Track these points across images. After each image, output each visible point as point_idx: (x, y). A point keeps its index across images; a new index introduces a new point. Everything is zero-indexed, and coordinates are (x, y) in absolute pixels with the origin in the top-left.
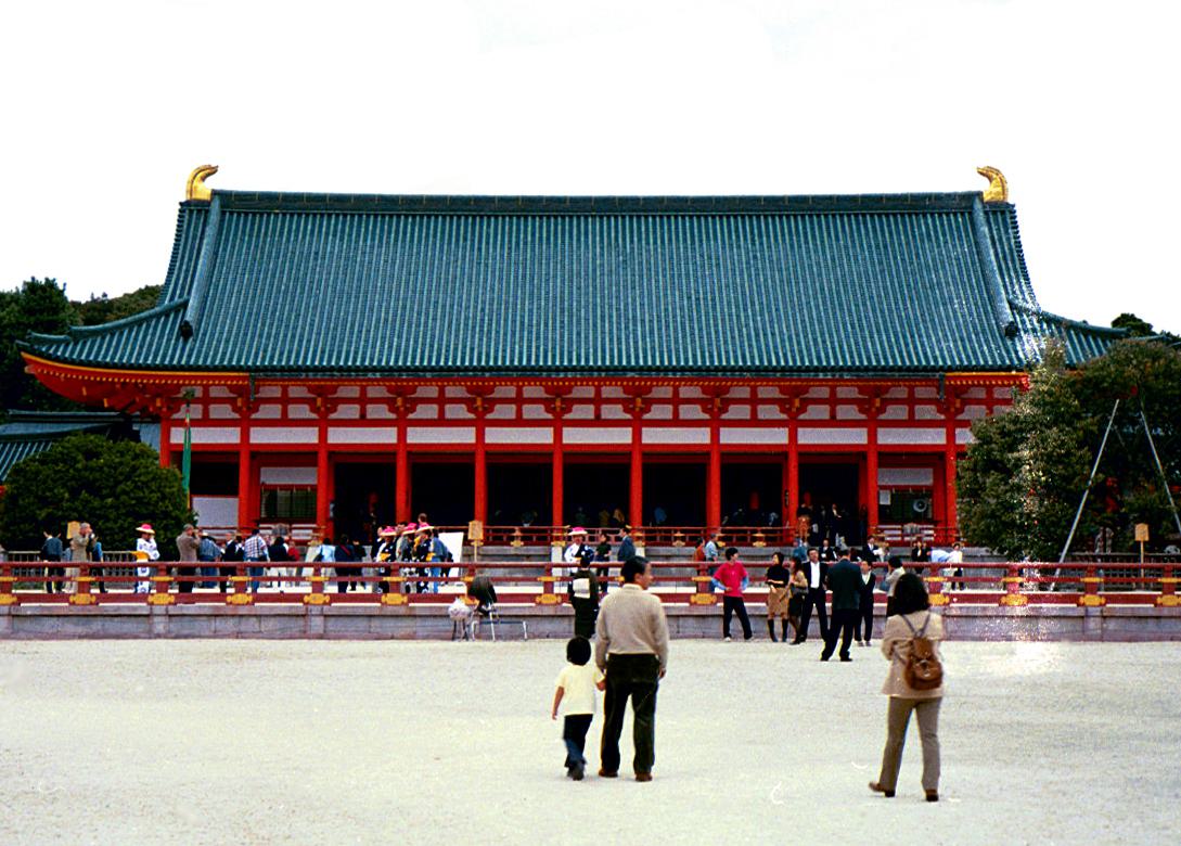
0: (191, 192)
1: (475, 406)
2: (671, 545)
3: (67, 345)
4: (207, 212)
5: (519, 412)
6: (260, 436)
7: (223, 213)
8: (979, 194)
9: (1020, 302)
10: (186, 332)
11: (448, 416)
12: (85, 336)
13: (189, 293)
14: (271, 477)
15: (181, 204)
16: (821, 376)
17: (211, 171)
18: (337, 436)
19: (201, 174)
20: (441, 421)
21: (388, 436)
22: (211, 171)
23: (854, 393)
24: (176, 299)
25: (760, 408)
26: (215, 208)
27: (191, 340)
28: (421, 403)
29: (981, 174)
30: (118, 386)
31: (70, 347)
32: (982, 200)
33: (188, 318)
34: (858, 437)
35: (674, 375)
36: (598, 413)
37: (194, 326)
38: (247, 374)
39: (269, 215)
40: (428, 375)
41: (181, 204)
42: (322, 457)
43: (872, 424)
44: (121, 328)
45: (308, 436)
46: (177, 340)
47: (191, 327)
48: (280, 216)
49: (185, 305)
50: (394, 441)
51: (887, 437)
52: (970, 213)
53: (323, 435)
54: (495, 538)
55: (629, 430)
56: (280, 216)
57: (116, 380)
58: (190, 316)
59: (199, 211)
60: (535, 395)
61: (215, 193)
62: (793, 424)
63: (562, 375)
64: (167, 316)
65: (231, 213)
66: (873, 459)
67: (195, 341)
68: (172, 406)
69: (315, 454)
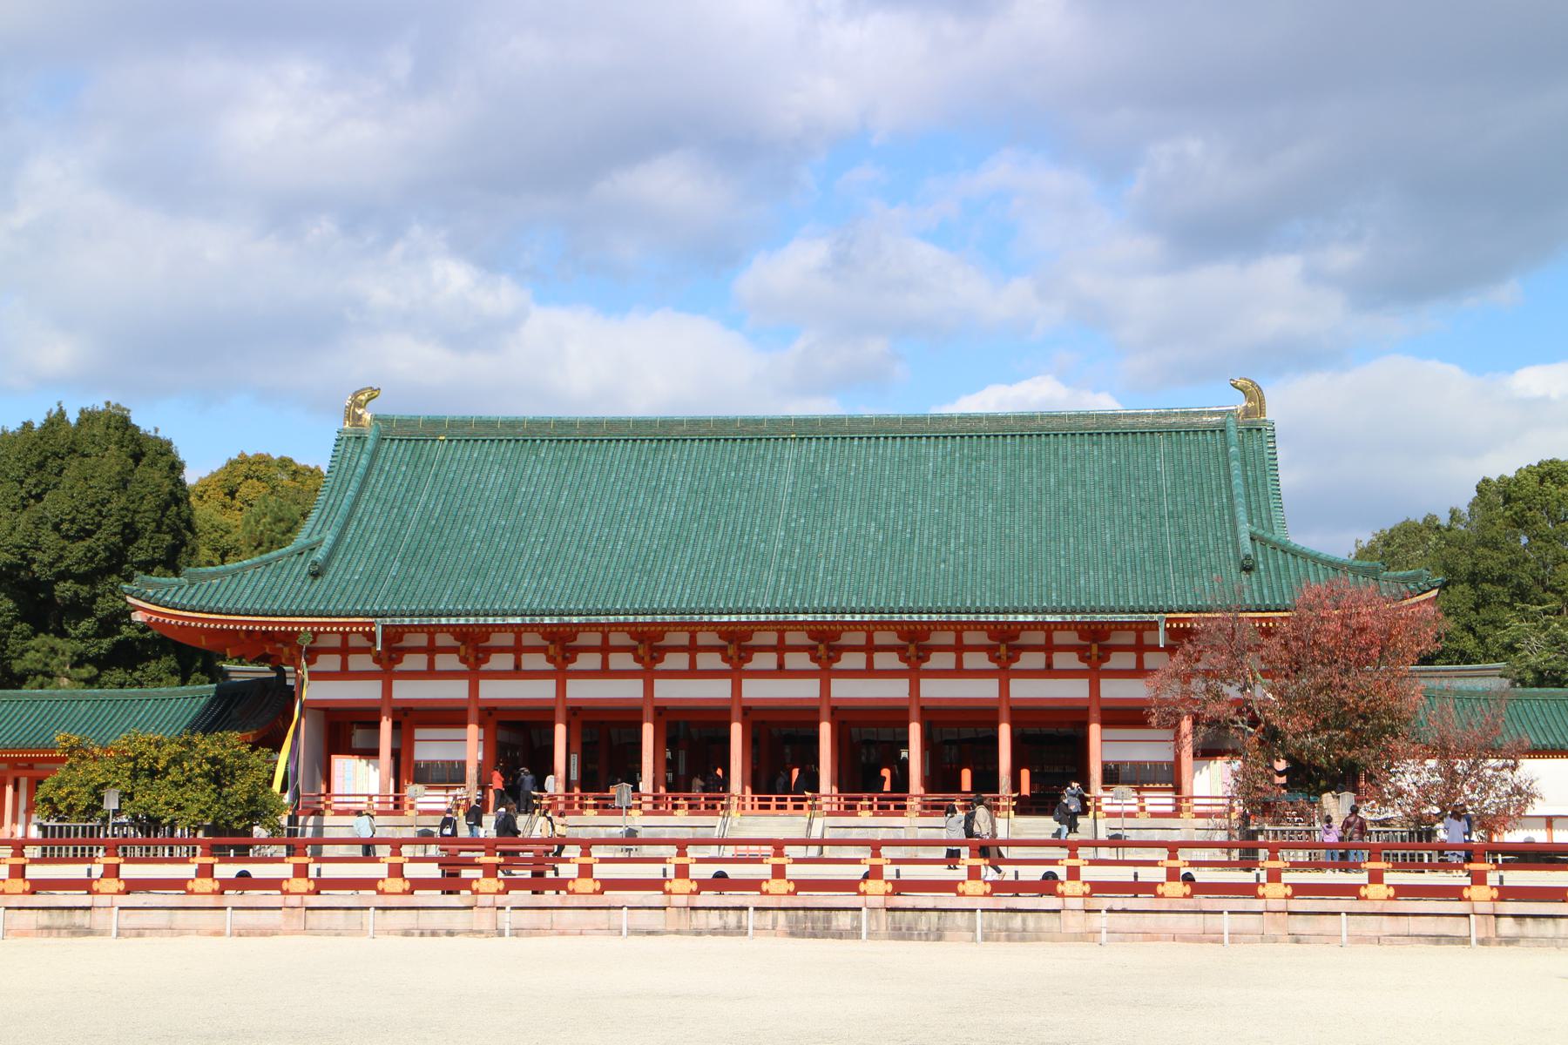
1: (818, 654)
2: (856, 815)
3: (181, 588)
5: (693, 662)
6: (405, 691)
9: (1260, 532)
12: (203, 577)
18: (492, 690)
20: (605, 672)
22: (374, 393)
23: (1071, 638)
27: (319, 580)
28: (670, 651)
30: (242, 636)
34: (1076, 689)
44: (244, 569)
45: (456, 690)
49: (320, 542)
50: (728, 695)
51: (1113, 689)
54: (847, 807)
57: (354, 629)
66: (1095, 715)
68: (480, 655)
69: (465, 711)
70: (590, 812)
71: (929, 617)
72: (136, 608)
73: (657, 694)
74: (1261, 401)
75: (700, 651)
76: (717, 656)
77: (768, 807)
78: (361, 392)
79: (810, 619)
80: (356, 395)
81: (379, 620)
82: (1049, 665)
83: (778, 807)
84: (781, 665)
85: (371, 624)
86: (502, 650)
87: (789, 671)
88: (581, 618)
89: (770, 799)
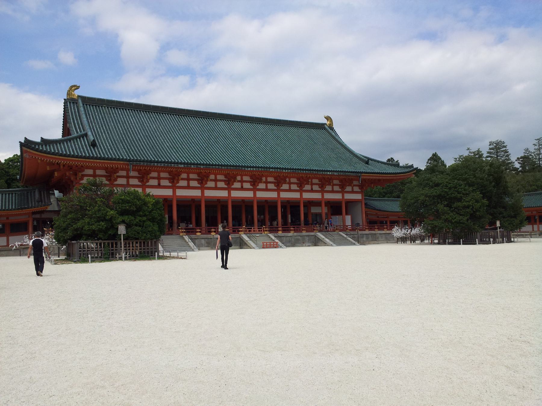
0: (68, 94)
7: (83, 104)
8: (326, 124)
16: (328, 173)
17: (78, 87)
19: (73, 88)
20: (188, 187)
25: (292, 185)
27: (96, 148)
29: (325, 118)
35: (285, 171)
36: (242, 187)
38: (128, 163)
40: (202, 167)
49: (86, 135)
60: (222, 179)
61: (79, 96)
62: (278, 190)
63: (249, 169)
70: (198, 234)
71: (305, 172)
72: (26, 152)
74: (332, 123)
75: (218, 181)
76: (223, 183)
78: (74, 86)
80: (72, 87)
85: (128, 165)
86: (154, 178)
87: (244, 188)
88: (204, 166)
89: (251, 228)
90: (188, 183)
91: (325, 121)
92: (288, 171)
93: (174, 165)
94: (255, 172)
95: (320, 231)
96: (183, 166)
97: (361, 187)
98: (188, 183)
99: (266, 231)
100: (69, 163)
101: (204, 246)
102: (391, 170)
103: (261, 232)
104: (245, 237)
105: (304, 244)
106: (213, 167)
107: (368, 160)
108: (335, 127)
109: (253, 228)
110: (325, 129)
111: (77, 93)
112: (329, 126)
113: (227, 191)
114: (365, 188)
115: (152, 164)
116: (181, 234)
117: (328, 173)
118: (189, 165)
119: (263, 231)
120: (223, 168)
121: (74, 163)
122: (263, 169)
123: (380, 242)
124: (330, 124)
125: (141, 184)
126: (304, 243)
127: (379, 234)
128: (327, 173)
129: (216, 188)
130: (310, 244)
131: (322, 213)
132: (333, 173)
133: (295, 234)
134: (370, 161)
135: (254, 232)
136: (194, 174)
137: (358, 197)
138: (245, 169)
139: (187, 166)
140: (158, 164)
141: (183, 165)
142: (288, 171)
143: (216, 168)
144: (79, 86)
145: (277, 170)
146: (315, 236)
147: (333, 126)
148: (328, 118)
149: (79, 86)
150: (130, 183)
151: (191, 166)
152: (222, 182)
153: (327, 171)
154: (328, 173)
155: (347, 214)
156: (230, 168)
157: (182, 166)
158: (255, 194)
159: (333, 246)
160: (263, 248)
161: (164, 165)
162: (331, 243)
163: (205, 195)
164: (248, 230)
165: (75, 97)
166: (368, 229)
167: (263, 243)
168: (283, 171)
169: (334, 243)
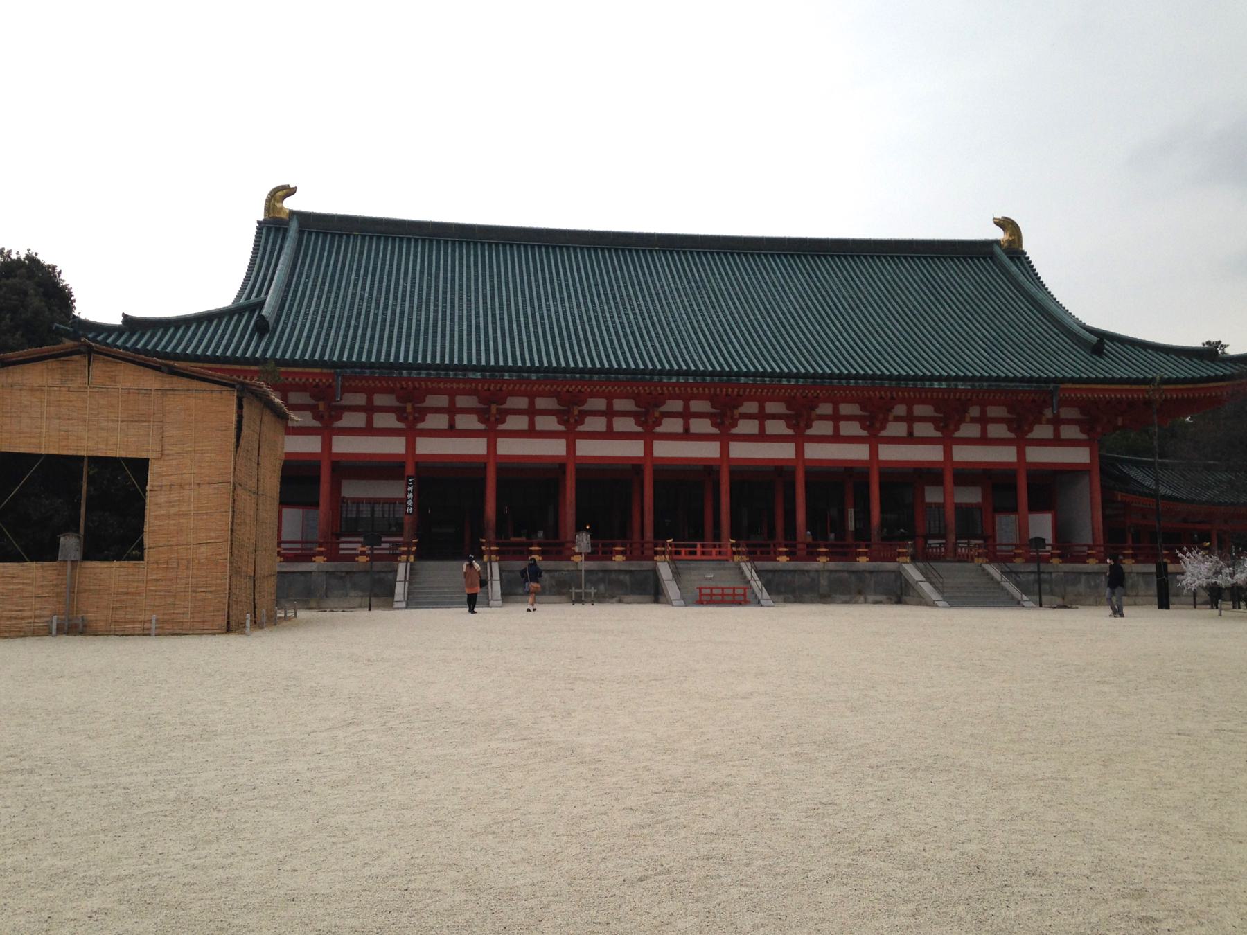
2: (775, 560)
4: (286, 230)
6: (344, 446)
7: (301, 232)
8: (997, 242)
10: (263, 328)
11: (539, 427)
13: (267, 293)
14: (352, 490)
15: (259, 222)
16: (936, 385)
17: (289, 191)
18: (427, 447)
19: (280, 193)
21: (476, 447)
22: (289, 191)
24: (253, 298)
25: (842, 424)
26: (294, 227)
31: (125, 337)
32: (1001, 246)
33: (263, 313)
34: (933, 454)
37: (271, 323)
38: (332, 371)
39: (348, 236)
40: (534, 377)
41: (259, 222)
42: (410, 470)
43: (948, 441)
45: (395, 446)
46: (252, 336)
47: (267, 322)
48: (359, 237)
49: (262, 303)
52: (991, 258)
53: (411, 445)
55: (718, 444)
56: (359, 237)
58: (266, 311)
59: (277, 230)
61: (293, 213)
64: (241, 316)
65: (310, 233)
66: (949, 479)
67: (272, 338)
73: (578, 453)
77: (694, 553)
79: (750, 382)
81: (338, 370)
82: (910, 433)
83: (703, 553)
84: (687, 429)
86: (437, 410)
90: (532, 423)
91: (998, 234)
92: (797, 382)
93: (455, 375)
94: (795, 391)
95: (914, 559)
96: (480, 377)
97: (1088, 424)
98: (532, 423)
99: (738, 553)
100: (307, 380)
101: (547, 593)
102: (1206, 370)
103: (725, 557)
104: (665, 570)
105: (862, 598)
106: (565, 377)
107: (1101, 342)
108: (1026, 247)
109: (699, 546)
110: (992, 256)
111: (290, 204)
112: (1010, 245)
113: (642, 442)
114: (1099, 430)
115: (395, 374)
116: (485, 558)
117: (936, 383)
118: (497, 374)
119: (729, 553)
120: (596, 377)
121: (317, 380)
122: (716, 379)
123: (1139, 600)
124: (1008, 241)
125: (404, 427)
126: (860, 592)
127: (1138, 573)
128: (932, 385)
129: (610, 434)
130: (879, 598)
131: (944, 504)
132: (952, 383)
133: (832, 565)
134: (1108, 345)
135: (704, 557)
136: (549, 399)
137: (1080, 456)
138: (661, 380)
139: (490, 376)
140: (410, 374)
141: (479, 374)
142: (797, 382)
143: (574, 379)
144: (296, 188)
145: (761, 381)
146: (899, 574)
147: (1021, 246)
148: (1006, 224)
149: (296, 188)
150: (375, 425)
151: (503, 376)
152: (628, 418)
153: (932, 378)
154: (936, 385)
155: (1035, 507)
156: (617, 378)
157: (479, 375)
158: (648, 449)
159: (937, 606)
160: (700, 602)
161: (429, 374)
162: (935, 596)
163: (578, 453)
164: (683, 550)
165: (284, 216)
166: (1133, 558)
167: (700, 589)
168: (780, 381)
169: (945, 599)
